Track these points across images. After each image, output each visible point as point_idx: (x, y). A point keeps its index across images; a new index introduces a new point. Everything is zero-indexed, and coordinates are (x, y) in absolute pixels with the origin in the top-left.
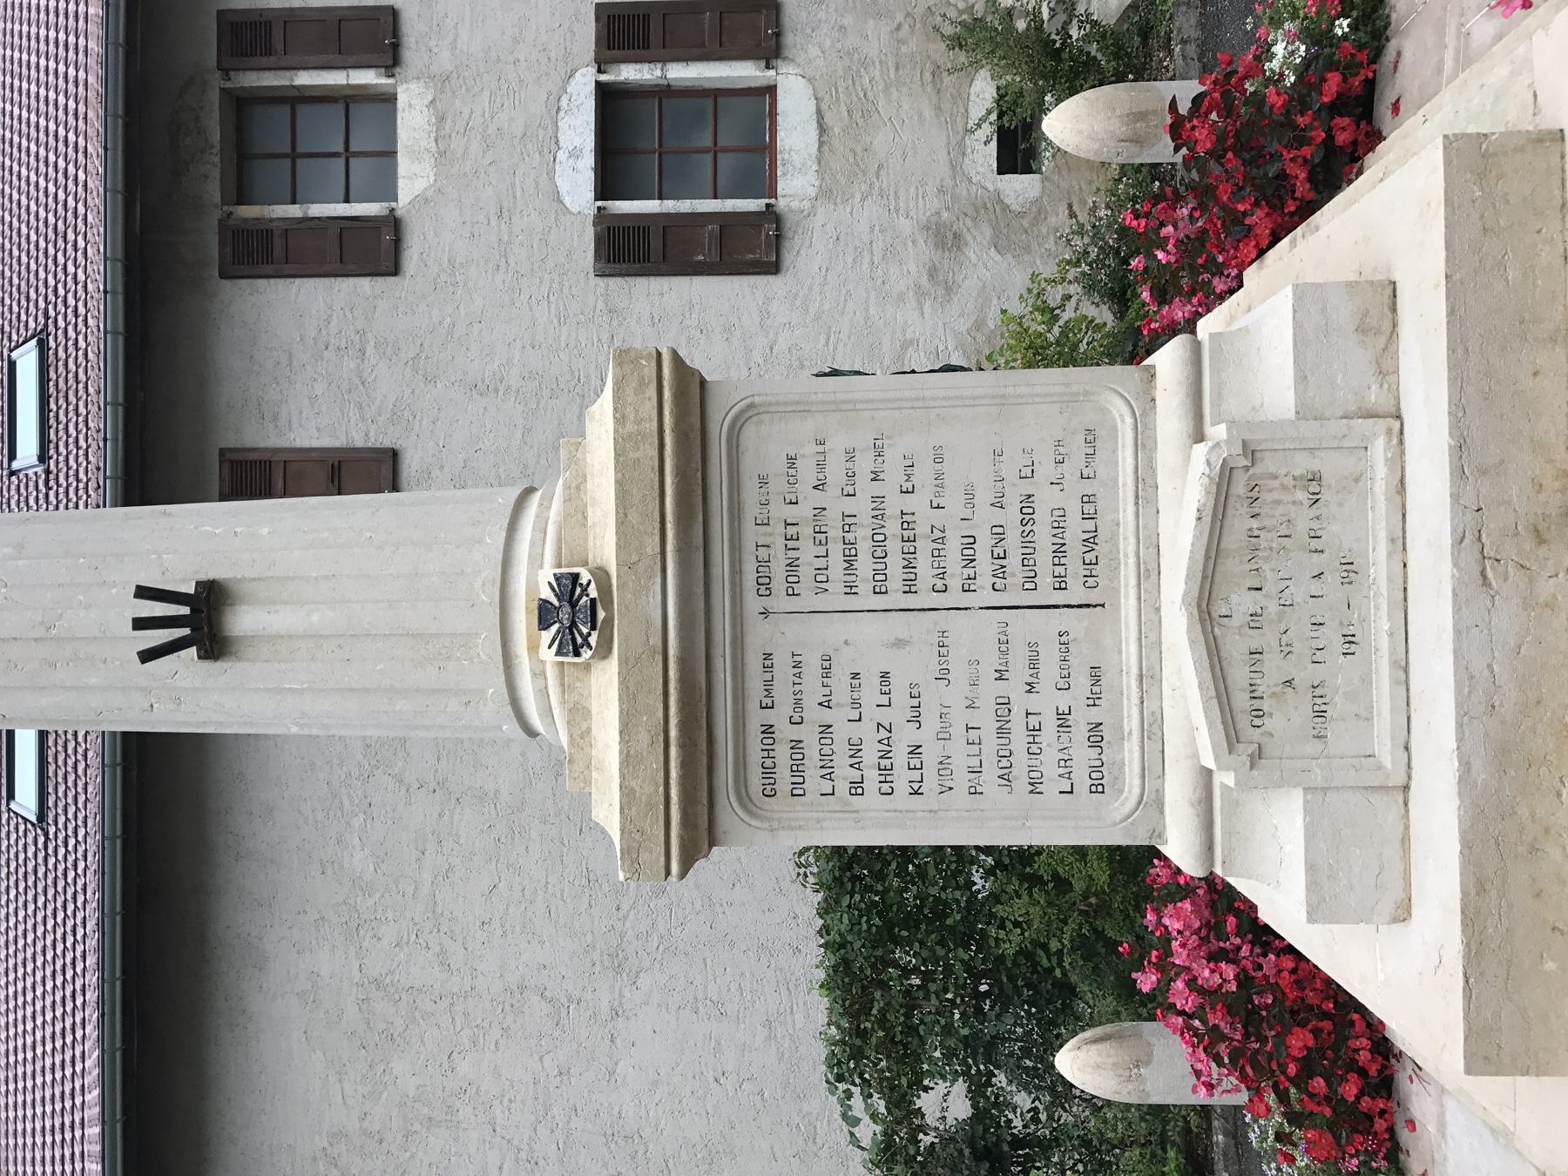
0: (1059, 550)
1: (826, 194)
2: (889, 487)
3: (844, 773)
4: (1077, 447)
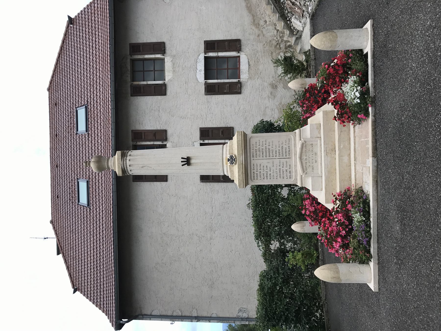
0: (286, 152)
1: (250, 78)
2: (267, 145)
3: (262, 177)
4: (288, 141)
